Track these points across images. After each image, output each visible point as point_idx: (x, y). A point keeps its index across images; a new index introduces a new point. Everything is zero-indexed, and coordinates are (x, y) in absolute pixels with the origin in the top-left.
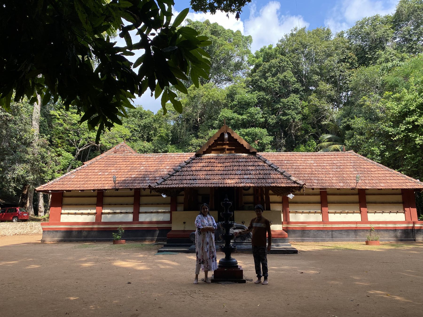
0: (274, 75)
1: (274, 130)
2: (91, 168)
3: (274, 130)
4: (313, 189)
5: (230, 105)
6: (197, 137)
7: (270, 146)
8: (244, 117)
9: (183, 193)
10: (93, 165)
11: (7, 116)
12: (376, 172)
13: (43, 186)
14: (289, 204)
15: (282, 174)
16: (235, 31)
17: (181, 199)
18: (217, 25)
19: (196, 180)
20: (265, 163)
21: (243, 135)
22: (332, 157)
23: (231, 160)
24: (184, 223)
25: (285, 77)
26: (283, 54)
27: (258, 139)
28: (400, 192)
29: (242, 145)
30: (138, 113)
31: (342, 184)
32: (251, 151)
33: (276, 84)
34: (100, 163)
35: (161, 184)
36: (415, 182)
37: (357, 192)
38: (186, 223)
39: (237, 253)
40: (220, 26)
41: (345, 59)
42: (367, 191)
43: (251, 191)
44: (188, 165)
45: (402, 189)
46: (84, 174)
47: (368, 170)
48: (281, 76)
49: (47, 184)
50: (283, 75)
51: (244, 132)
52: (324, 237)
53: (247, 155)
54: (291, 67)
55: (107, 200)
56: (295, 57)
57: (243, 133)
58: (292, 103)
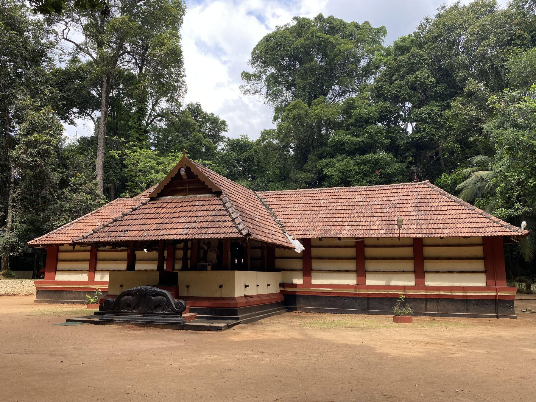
0: (402, 77)
1: (407, 154)
2: (93, 217)
3: (407, 154)
4: (340, 239)
5: (346, 124)
6: (304, 171)
7: (401, 177)
8: (361, 139)
9: (182, 245)
10: (97, 214)
11: (36, 161)
12: (448, 212)
13: (36, 239)
14: (313, 260)
15: (233, 220)
16: (360, 24)
17: (180, 254)
18: (333, 18)
19: (127, 231)
20: (224, 205)
21: (358, 164)
22: (394, 191)
23: (186, 204)
24: (121, 286)
25: (416, 77)
26: (420, 46)
27: (379, 169)
28: (480, 241)
29: (204, 182)
30: (237, 145)
31: (383, 232)
32: (214, 191)
33: (404, 89)
34: (106, 211)
35: (87, 237)
36: (502, 226)
37: (410, 242)
38: (123, 287)
39: (149, 326)
40: (337, 20)
41: (512, 40)
42: (425, 242)
43: (182, 245)
44: (133, 212)
45: (484, 237)
46: (83, 224)
47: (437, 208)
48: (411, 78)
49: (41, 237)
50: (414, 76)
51: (361, 160)
52: (356, 307)
53: (210, 195)
54: (428, 64)
55: (101, 255)
56: (434, 48)
57: (358, 161)
58: (428, 114)
